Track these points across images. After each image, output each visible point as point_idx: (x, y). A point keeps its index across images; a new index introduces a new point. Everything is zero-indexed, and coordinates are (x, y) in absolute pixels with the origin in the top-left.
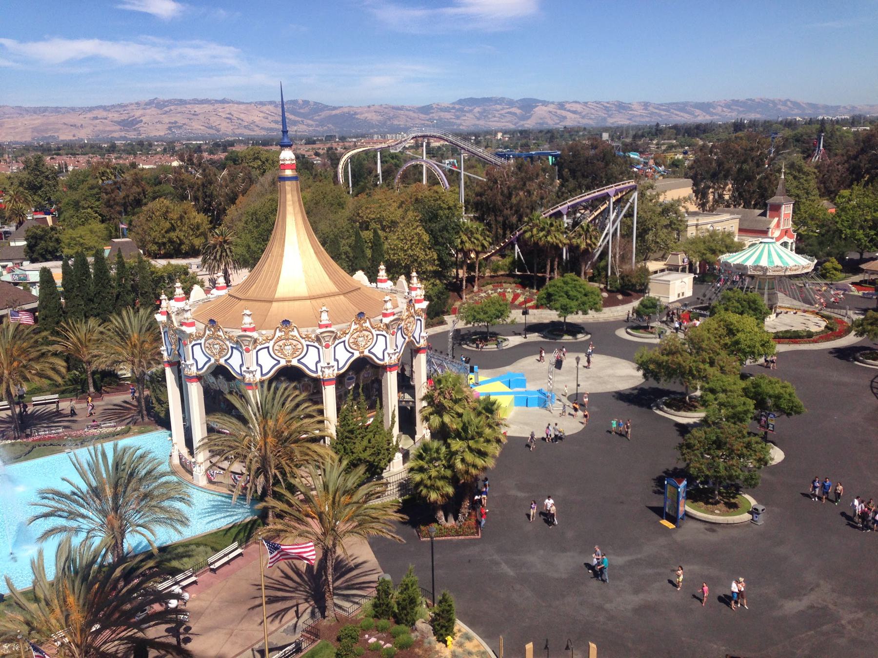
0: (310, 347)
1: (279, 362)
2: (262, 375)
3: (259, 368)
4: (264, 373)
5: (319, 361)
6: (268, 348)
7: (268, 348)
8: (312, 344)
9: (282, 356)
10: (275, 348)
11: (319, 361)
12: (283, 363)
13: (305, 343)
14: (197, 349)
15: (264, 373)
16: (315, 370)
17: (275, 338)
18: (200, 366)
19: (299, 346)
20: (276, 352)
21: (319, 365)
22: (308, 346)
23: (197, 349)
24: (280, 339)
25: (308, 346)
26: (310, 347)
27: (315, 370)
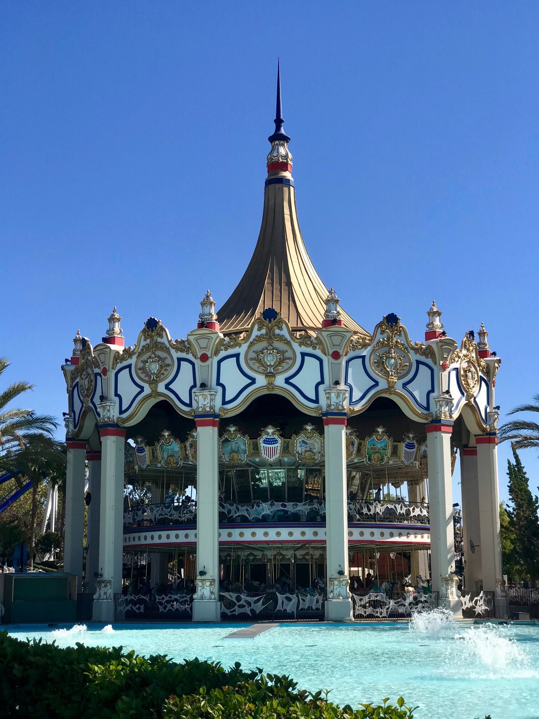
0: (306, 358)
1: (253, 381)
2: (224, 402)
3: (220, 389)
4: (227, 399)
5: (322, 382)
6: (237, 356)
7: (237, 356)
8: (309, 350)
9: (260, 370)
10: (249, 357)
11: (322, 382)
12: (261, 381)
13: (298, 349)
14: (124, 375)
15: (227, 399)
16: (314, 398)
17: (251, 340)
18: (124, 407)
19: (289, 354)
20: (251, 363)
21: (321, 388)
22: (303, 355)
23: (124, 375)
24: (259, 339)
25: (303, 355)
26: (306, 358)
27: (314, 398)
